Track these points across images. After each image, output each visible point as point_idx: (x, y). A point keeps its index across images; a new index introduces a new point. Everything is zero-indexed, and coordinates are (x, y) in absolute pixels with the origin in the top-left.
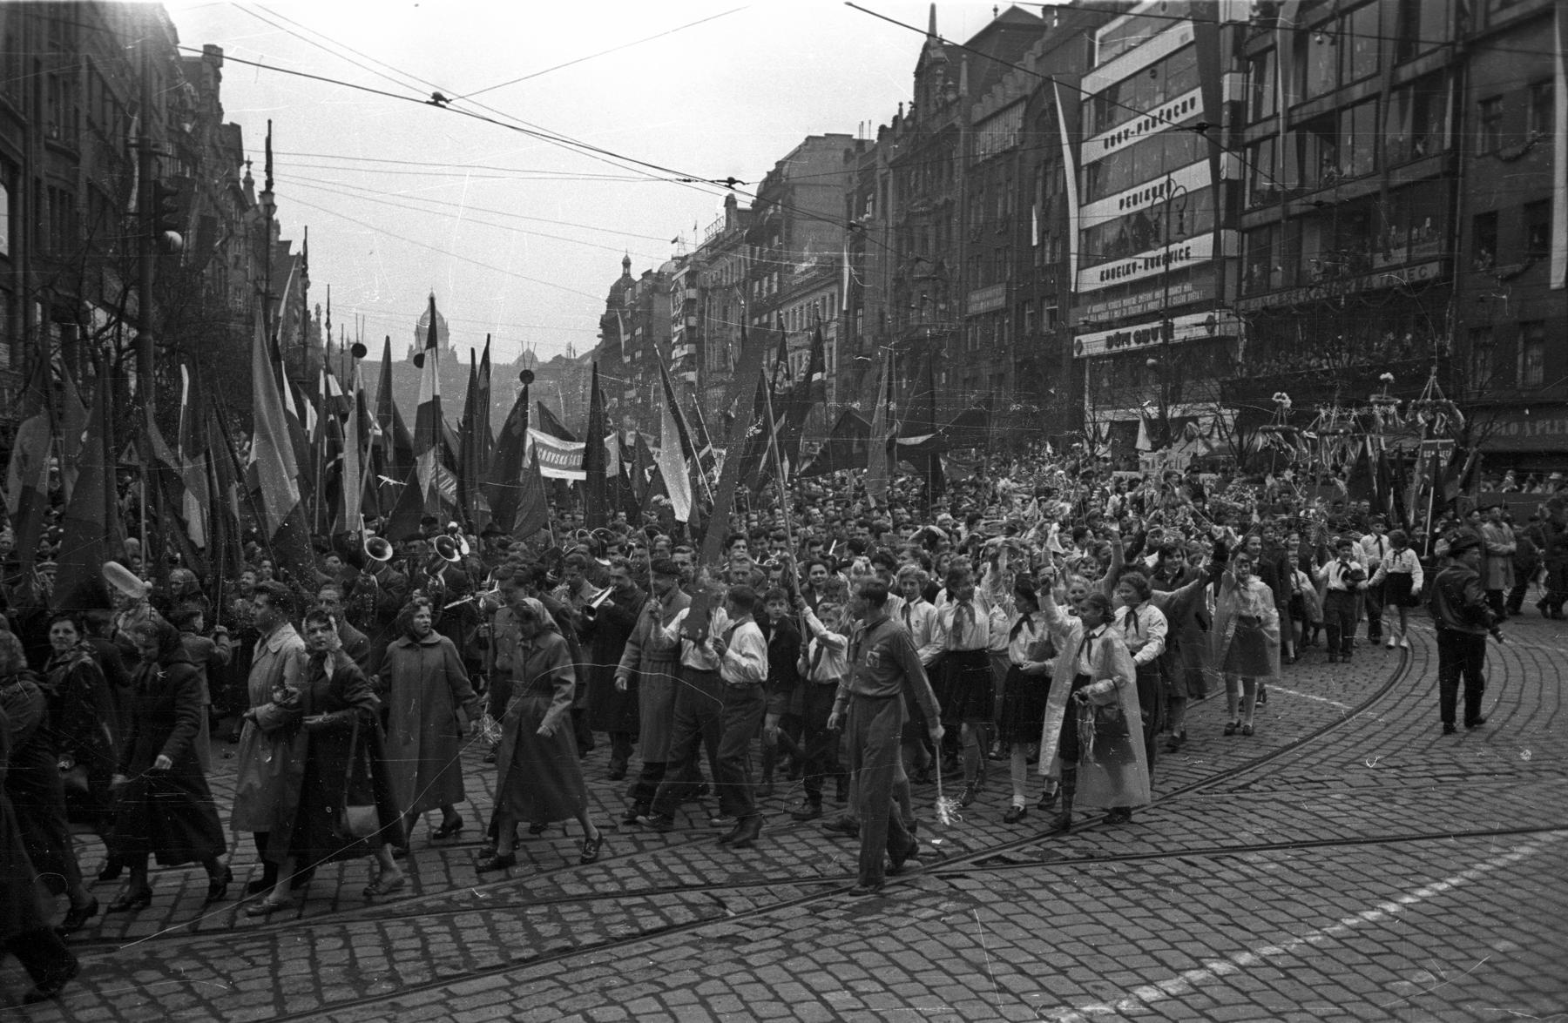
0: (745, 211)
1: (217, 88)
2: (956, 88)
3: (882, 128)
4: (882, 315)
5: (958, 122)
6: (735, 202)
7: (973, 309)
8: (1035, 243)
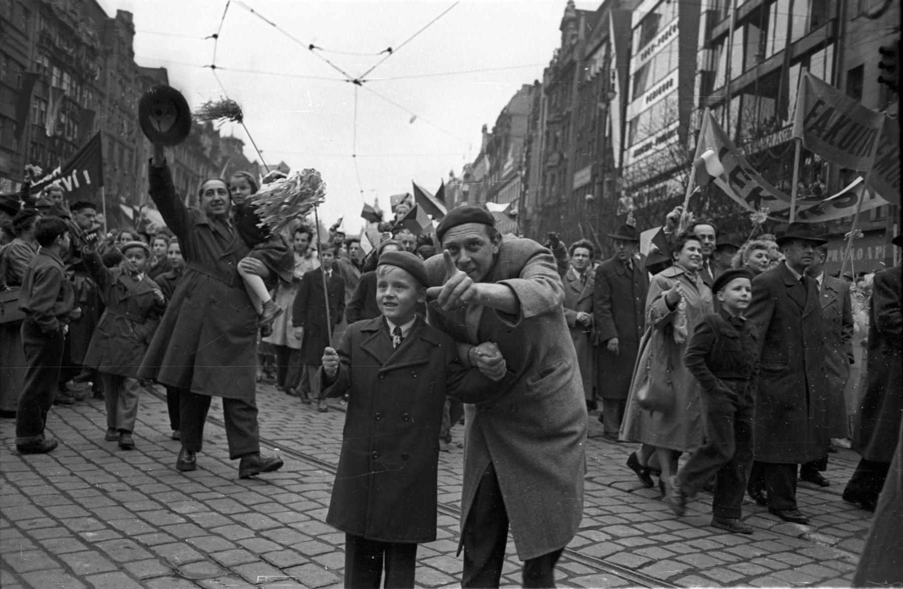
0: (489, 135)
1: (132, 39)
2: (577, 35)
3: (546, 70)
4: (537, 192)
5: (576, 57)
7: (577, 184)
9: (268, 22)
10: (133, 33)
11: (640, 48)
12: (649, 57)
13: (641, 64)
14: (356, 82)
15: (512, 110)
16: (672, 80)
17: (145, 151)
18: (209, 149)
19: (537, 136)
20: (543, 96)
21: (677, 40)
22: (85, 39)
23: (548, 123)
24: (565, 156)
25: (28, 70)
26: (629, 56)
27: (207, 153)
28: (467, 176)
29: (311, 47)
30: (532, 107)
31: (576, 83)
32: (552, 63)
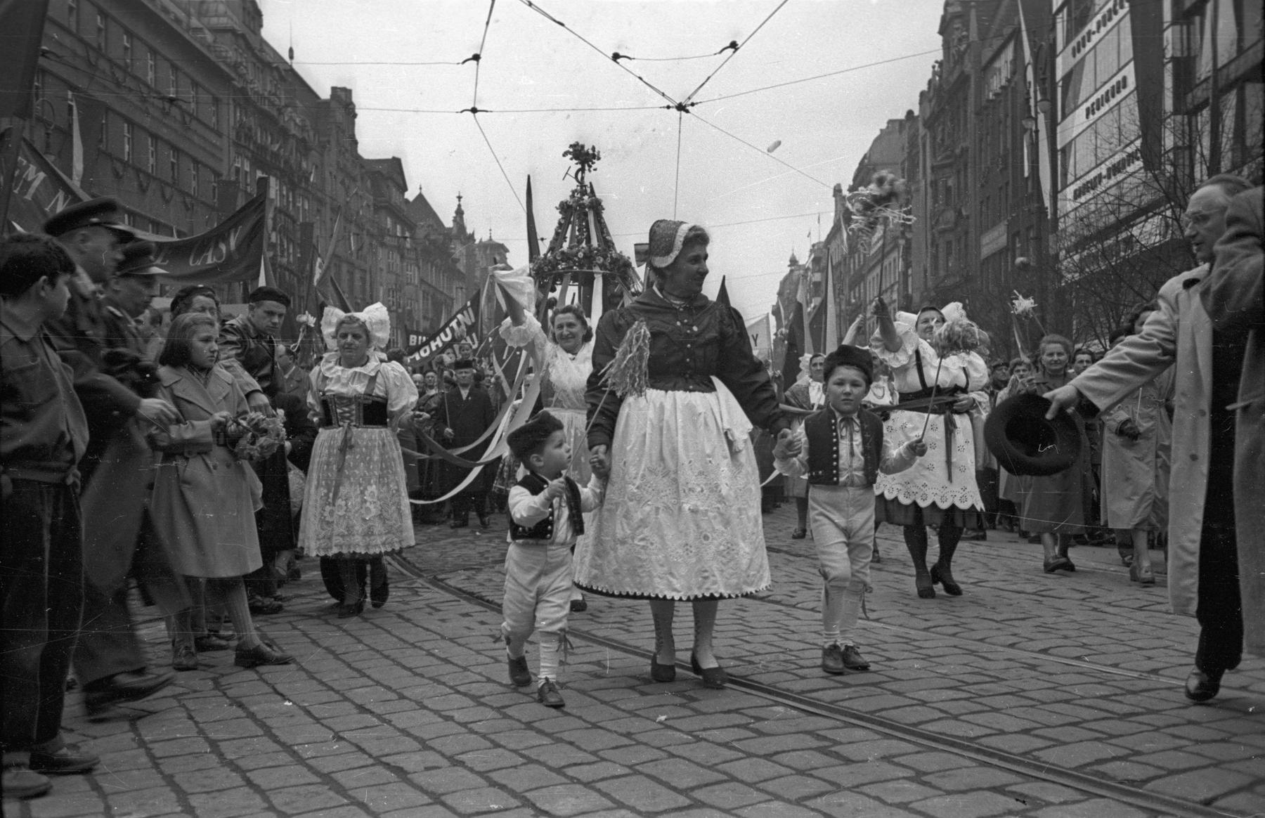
1: (353, 124)
2: (967, 37)
3: (922, 94)
5: (968, 67)
6: (840, 191)
7: (986, 251)
8: (1026, 174)
9: (555, 21)
10: (355, 116)
11: (1068, 42)
12: (1084, 51)
13: (1073, 62)
14: (681, 107)
15: (875, 158)
16: (1125, 79)
17: (381, 270)
18: (463, 261)
19: (917, 190)
20: (922, 131)
21: (1128, 18)
22: (294, 131)
23: (933, 168)
24: (964, 213)
25: (224, 178)
26: (1053, 54)
27: (461, 267)
28: (816, 261)
29: (616, 57)
30: (906, 150)
31: (971, 108)
32: (930, 82)
